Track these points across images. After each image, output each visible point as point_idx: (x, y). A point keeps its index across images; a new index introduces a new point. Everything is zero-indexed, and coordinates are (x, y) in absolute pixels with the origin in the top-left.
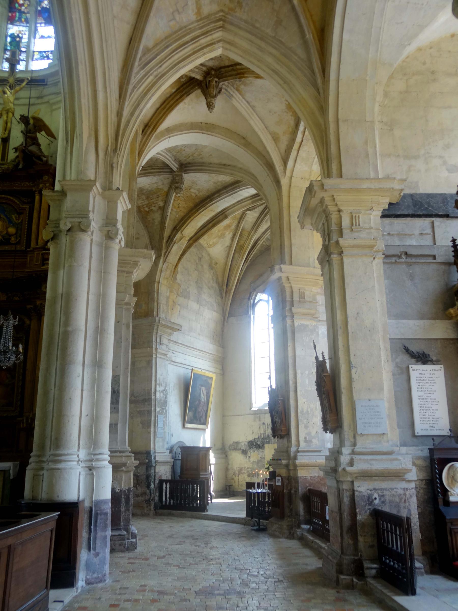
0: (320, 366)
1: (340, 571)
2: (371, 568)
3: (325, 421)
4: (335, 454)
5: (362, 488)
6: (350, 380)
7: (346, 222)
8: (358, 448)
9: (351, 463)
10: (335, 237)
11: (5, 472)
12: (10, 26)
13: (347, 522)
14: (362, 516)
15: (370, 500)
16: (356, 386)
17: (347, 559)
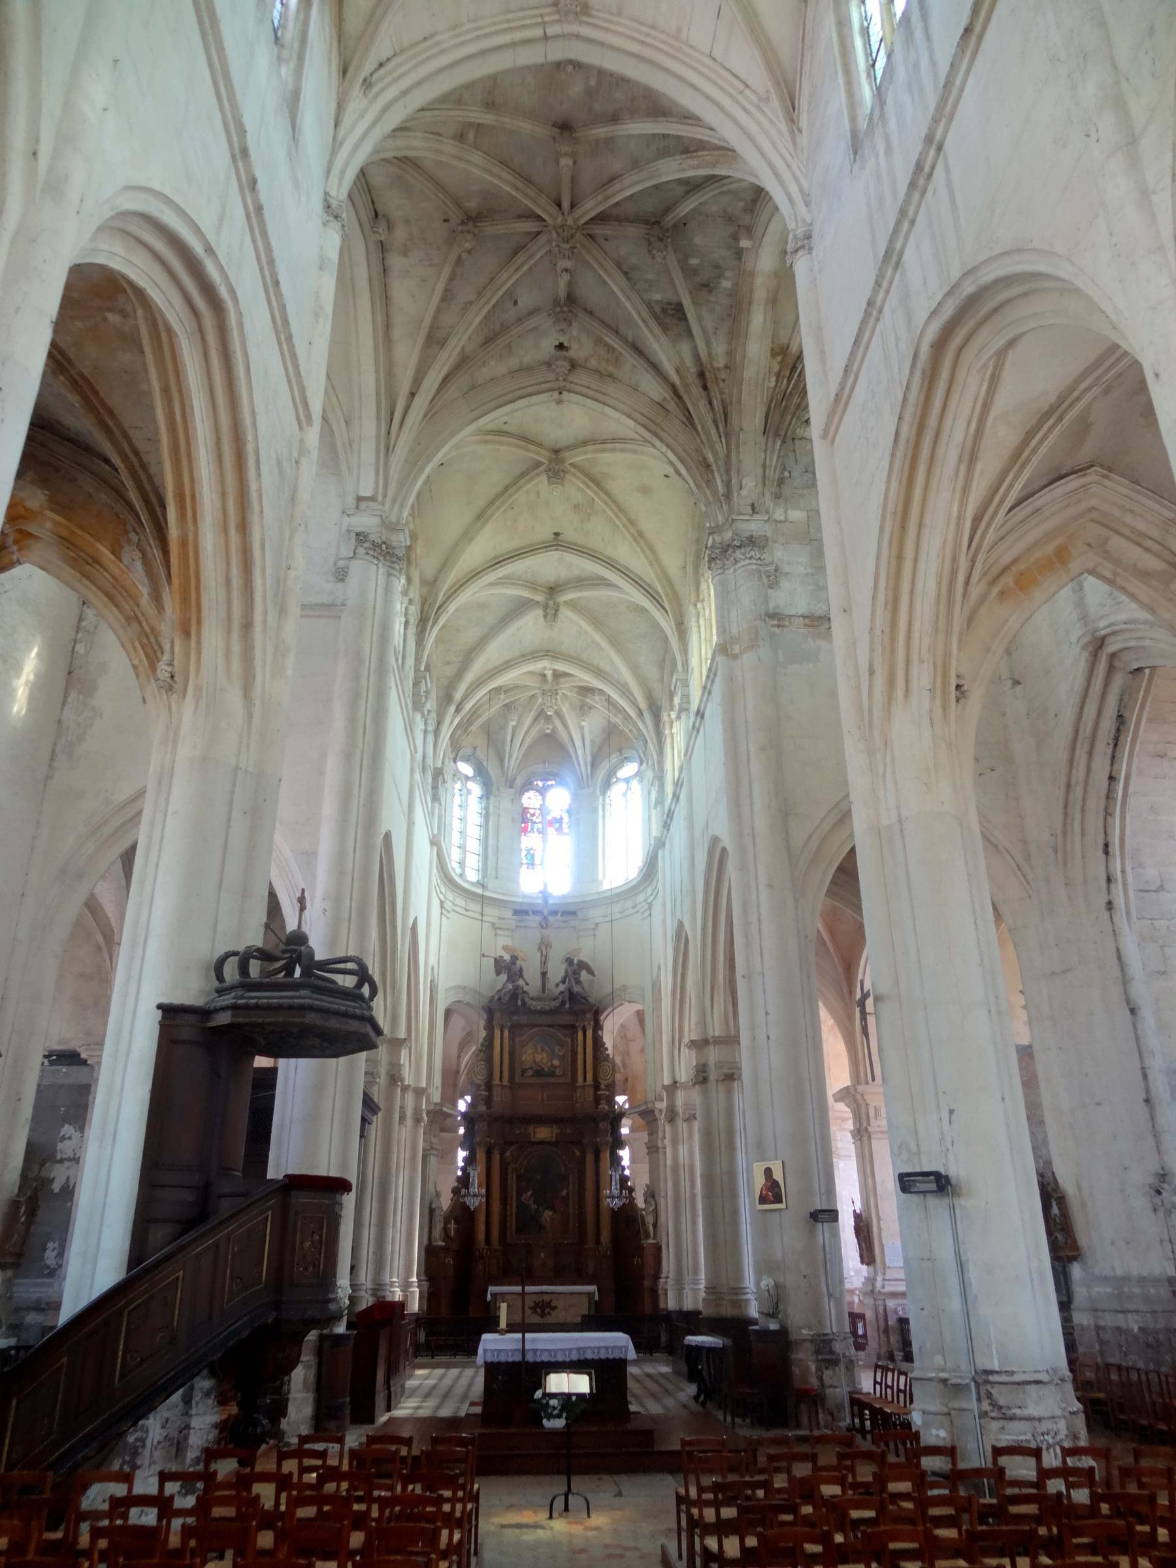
0: (858, 1217)
1: (879, 1359)
2: (899, 1355)
3: (861, 1257)
4: (871, 1281)
5: (891, 1304)
6: (880, 1229)
7: (872, 1113)
8: (887, 1277)
9: (883, 1287)
10: (865, 1124)
11: (590, 1295)
12: (523, 838)
13: (882, 1326)
14: (892, 1322)
15: (896, 1312)
16: (884, 1233)
17: (884, 1350)
